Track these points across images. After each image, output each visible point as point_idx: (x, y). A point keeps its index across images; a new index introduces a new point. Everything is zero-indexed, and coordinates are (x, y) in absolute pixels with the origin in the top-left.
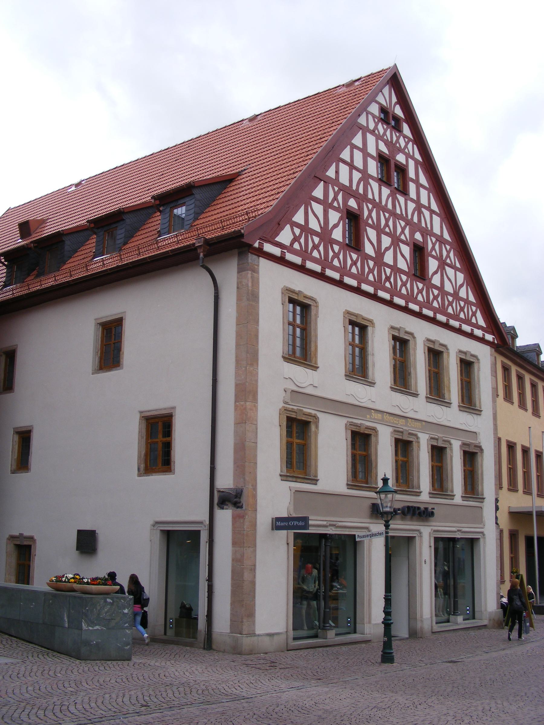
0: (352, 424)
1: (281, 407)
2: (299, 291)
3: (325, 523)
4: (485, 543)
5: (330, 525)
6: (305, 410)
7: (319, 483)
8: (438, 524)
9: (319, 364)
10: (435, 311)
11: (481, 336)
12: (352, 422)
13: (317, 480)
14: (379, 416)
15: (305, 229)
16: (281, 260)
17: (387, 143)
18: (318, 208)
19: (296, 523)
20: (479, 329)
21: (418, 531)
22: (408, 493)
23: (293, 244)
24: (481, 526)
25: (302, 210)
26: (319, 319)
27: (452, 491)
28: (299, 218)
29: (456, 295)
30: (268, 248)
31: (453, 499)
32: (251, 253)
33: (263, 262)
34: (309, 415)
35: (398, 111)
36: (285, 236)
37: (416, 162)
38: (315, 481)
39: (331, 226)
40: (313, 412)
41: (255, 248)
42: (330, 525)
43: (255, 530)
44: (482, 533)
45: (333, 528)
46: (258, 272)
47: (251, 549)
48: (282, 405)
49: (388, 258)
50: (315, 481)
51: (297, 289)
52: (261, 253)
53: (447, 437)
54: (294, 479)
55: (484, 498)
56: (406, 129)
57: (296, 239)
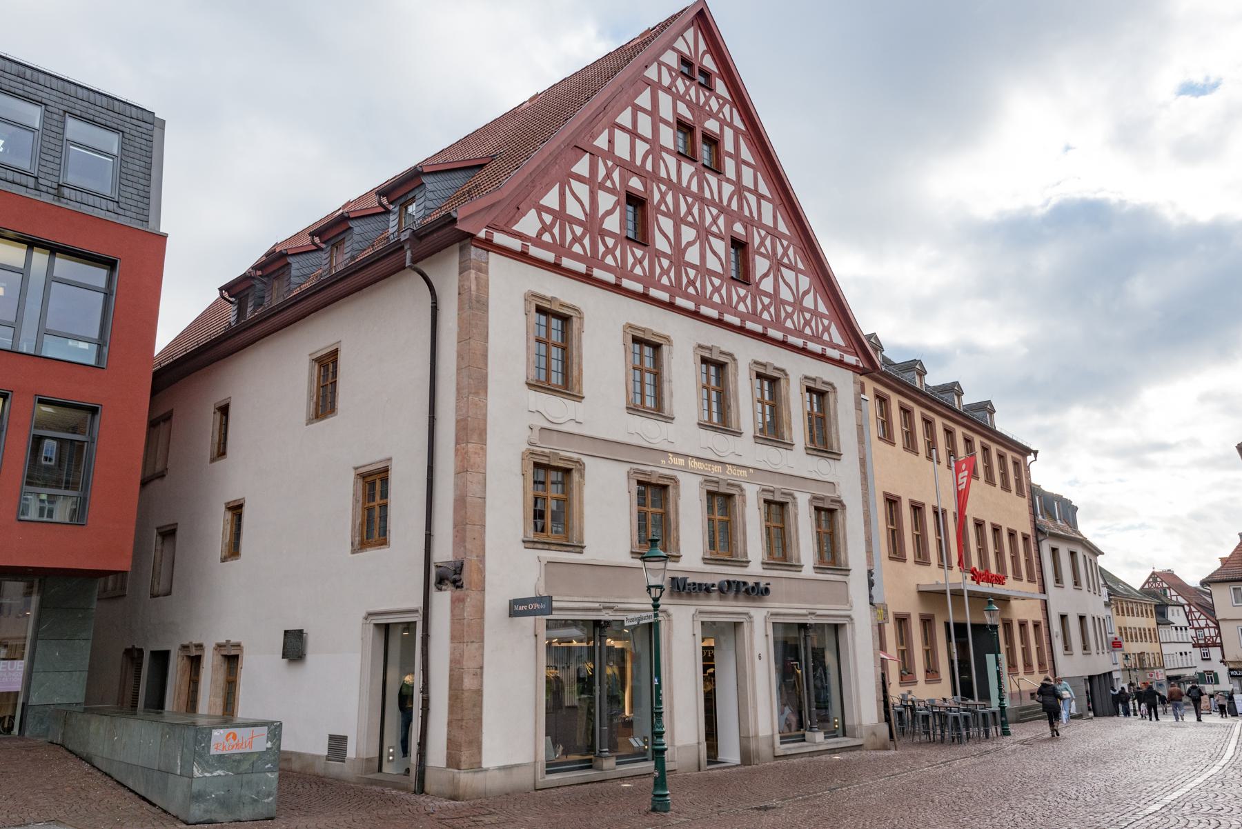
0: (637, 472)
3: (596, 605)
4: (853, 630)
5: (605, 608)
6: (562, 453)
7: (585, 551)
8: (777, 605)
9: (586, 392)
10: (766, 325)
11: (838, 357)
13: (583, 547)
14: (681, 461)
15: (561, 215)
16: (523, 256)
17: (689, 104)
18: (582, 190)
19: (536, 606)
21: (747, 614)
25: (555, 190)
26: (584, 335)
27: (799, 560)
28: (551, 199)
29: (798, 304)
30: (499, 238)
33: (493, 257)
34: (570, 460)
35: (709, 63)
36: (529, 224)
37: (737, 131)
38: (580, 548)
39: (601, 212)
40: (575, 456)
41: (479, 240)
42: (605, 608)
43: (482, 618)
44: (849, 616)
45: (610, 612)
46: (487, 272)
47: (475, 645)
48: (525, 447)
49: (692, 255)
50: (580, 548)
51: (549, 295)
52: (488, 245)
53: (787, 487)
56: (720, 87)
57: (545, 228)
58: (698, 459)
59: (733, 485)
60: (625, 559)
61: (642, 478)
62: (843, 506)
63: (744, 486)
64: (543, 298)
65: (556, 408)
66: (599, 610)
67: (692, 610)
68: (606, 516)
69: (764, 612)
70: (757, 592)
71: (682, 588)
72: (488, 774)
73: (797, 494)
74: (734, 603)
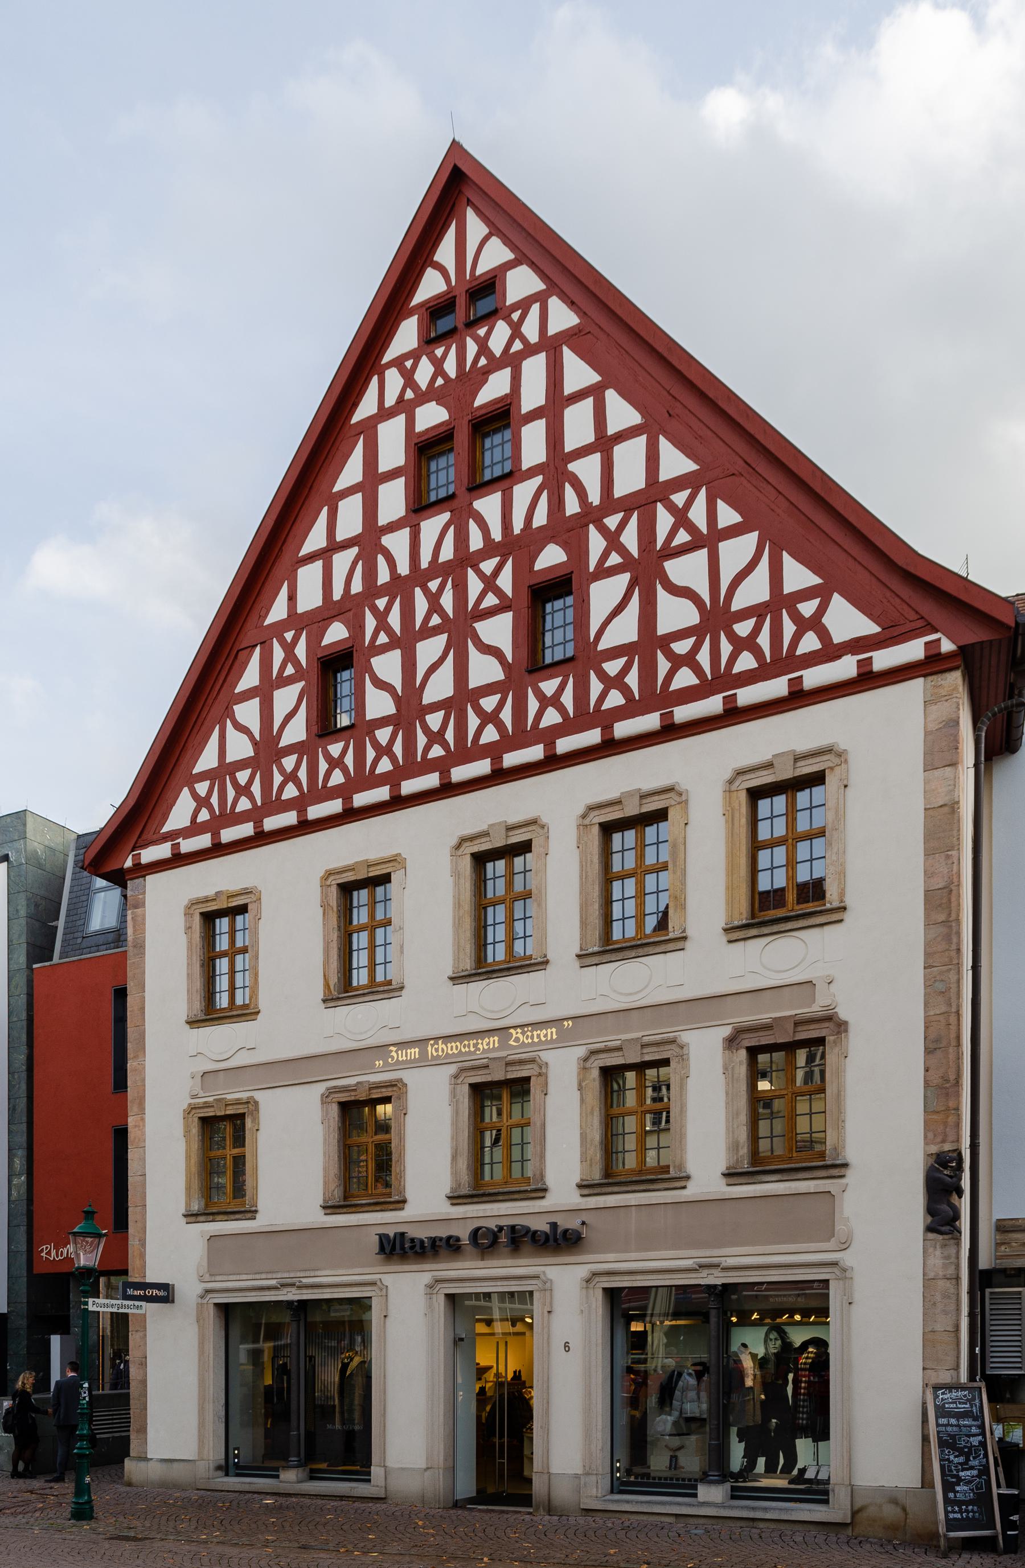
1: (185, 1106)
2: (217, 893)
3: (273, 1282)
5: (283, 1285)
6: (229, 1097)
7: (258, 1216)
8: (611, 1256)
12: (335, 1087)
13: (256, 1211)
14: (414, 1052)
20: (839, 657)
22: (516, 1196)
23: (196, 817)
24: (831, 1245)
31: (684, 1187)
32: (131, 879)
34: (238, 1102)
36: (181, 812)
40: (244, 1096)
41: (129, 870)
42: (283, 1285)
45: (294, 1290)
47: (141, 1334)
48: (186, 1102)
50: (251, 1213)
51: (210, 892)
53: (653, 1033)
54: (211, 1218)
55: (845, 1165)
57: (202, 802)
58: (448, 1038)
59: (521, 1062)
60: (321, 1219)
61: (344, 1097)
62: (841, 1027)
63: (545, 1056)
64: (207, 900)
65: (223, 1041)
66: (275, 1288)
67: (426, 1278)
68: (292, 1163)
69: (582, 1272)
70: (561, 1241)
71: (398, 1249)
72: (151, 1464)
73: (685, 1037)
74: (509, 1262)
